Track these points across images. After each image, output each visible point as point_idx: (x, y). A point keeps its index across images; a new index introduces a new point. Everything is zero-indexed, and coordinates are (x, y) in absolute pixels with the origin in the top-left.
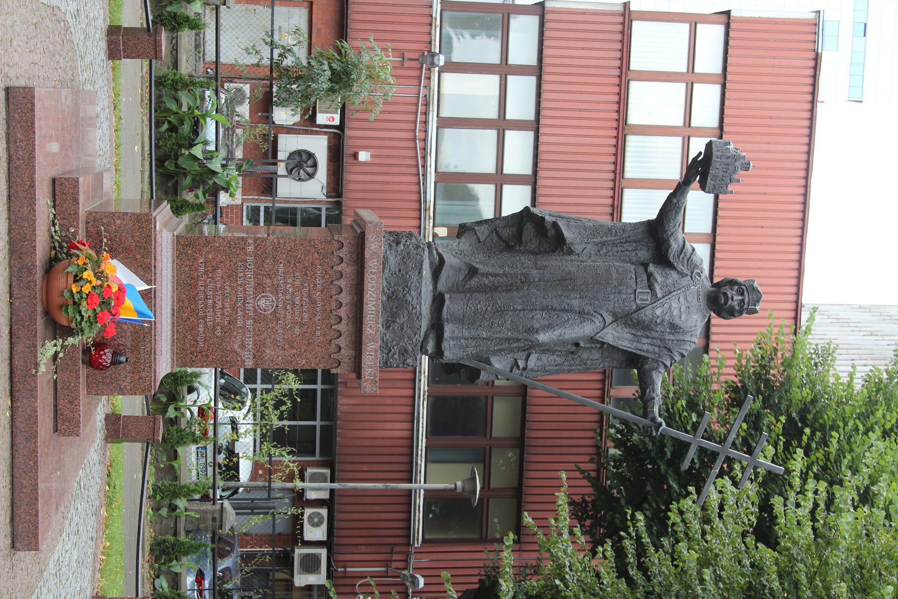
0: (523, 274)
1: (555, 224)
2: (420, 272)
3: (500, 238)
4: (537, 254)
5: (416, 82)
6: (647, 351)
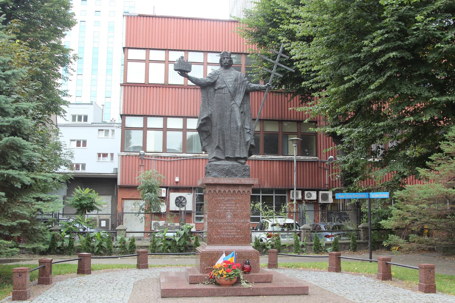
0: (219, 130)
1: (202, 120)
2: (218, 165)
3: (206, 138)
4: (212, 126)
5: (150, 161)
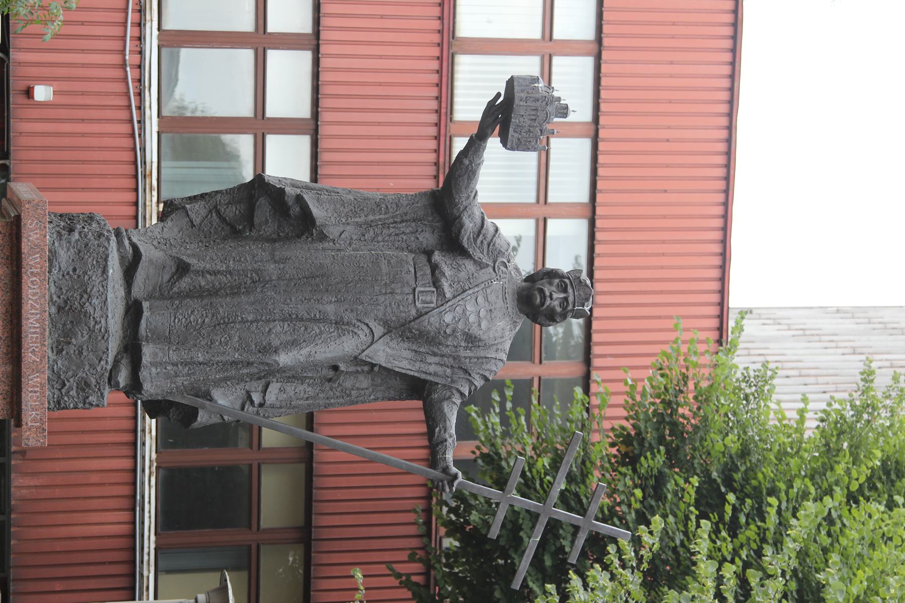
0: (257, 271)
1: (299, 199)
2: (105, 271)
3: (222, 219)
4: (274, 241)
6: (435, 374)
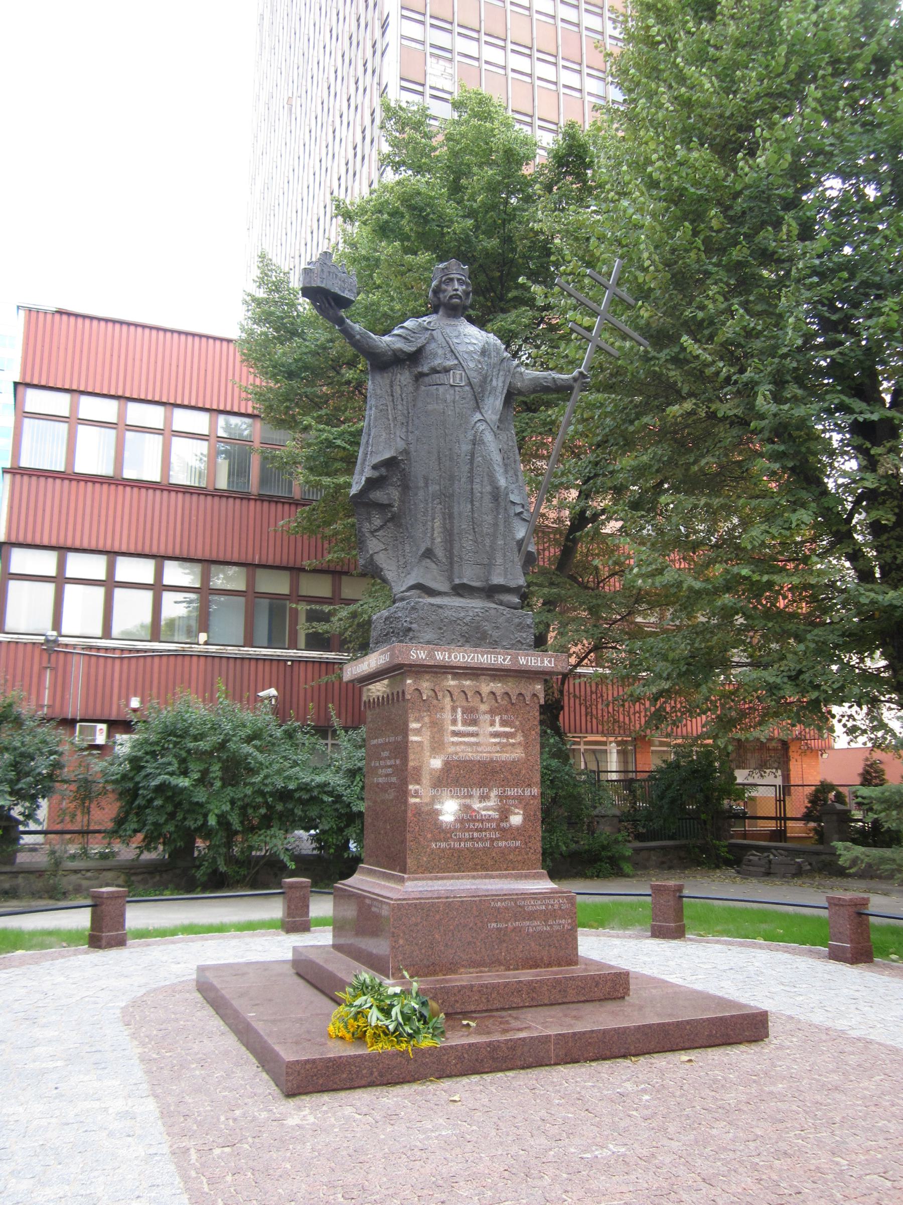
1: (375, 467)
2: (440, 607)
5: (69, 656)
6: (504, 382)
